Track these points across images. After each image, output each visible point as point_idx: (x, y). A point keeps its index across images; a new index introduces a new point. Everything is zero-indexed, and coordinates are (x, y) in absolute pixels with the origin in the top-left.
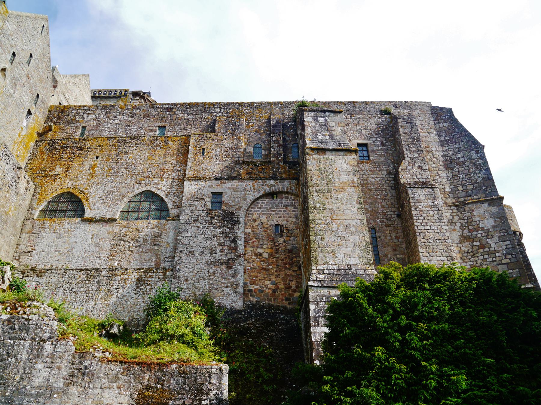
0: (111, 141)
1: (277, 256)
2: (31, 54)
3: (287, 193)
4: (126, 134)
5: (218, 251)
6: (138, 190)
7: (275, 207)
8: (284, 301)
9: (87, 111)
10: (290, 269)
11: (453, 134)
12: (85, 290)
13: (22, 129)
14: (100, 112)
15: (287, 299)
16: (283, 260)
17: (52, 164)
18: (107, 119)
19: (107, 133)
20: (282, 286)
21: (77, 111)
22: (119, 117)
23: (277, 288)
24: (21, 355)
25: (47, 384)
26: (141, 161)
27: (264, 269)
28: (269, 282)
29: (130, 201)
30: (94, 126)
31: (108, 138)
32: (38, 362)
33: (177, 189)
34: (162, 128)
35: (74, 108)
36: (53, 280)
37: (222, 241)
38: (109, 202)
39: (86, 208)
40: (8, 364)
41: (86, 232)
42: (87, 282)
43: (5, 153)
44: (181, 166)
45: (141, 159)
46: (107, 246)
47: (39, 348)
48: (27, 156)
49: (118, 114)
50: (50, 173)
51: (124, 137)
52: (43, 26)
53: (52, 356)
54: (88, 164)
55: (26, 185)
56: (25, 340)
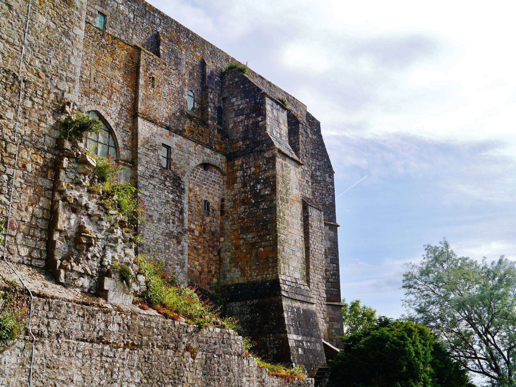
1: (204, 236)
3: (217, 168)
5: (171, 221)
7: (206, 181)
8: (207, 285)
10: (212, 253)
11: (317, 150)
15: (209, 284)
16: (208, 242)
20: (206, 270)
23: (203, 270)
27: (195, 248)
28: (197, 263)
33: (126, 122)
37: (174, 211)
44: (128, 90)
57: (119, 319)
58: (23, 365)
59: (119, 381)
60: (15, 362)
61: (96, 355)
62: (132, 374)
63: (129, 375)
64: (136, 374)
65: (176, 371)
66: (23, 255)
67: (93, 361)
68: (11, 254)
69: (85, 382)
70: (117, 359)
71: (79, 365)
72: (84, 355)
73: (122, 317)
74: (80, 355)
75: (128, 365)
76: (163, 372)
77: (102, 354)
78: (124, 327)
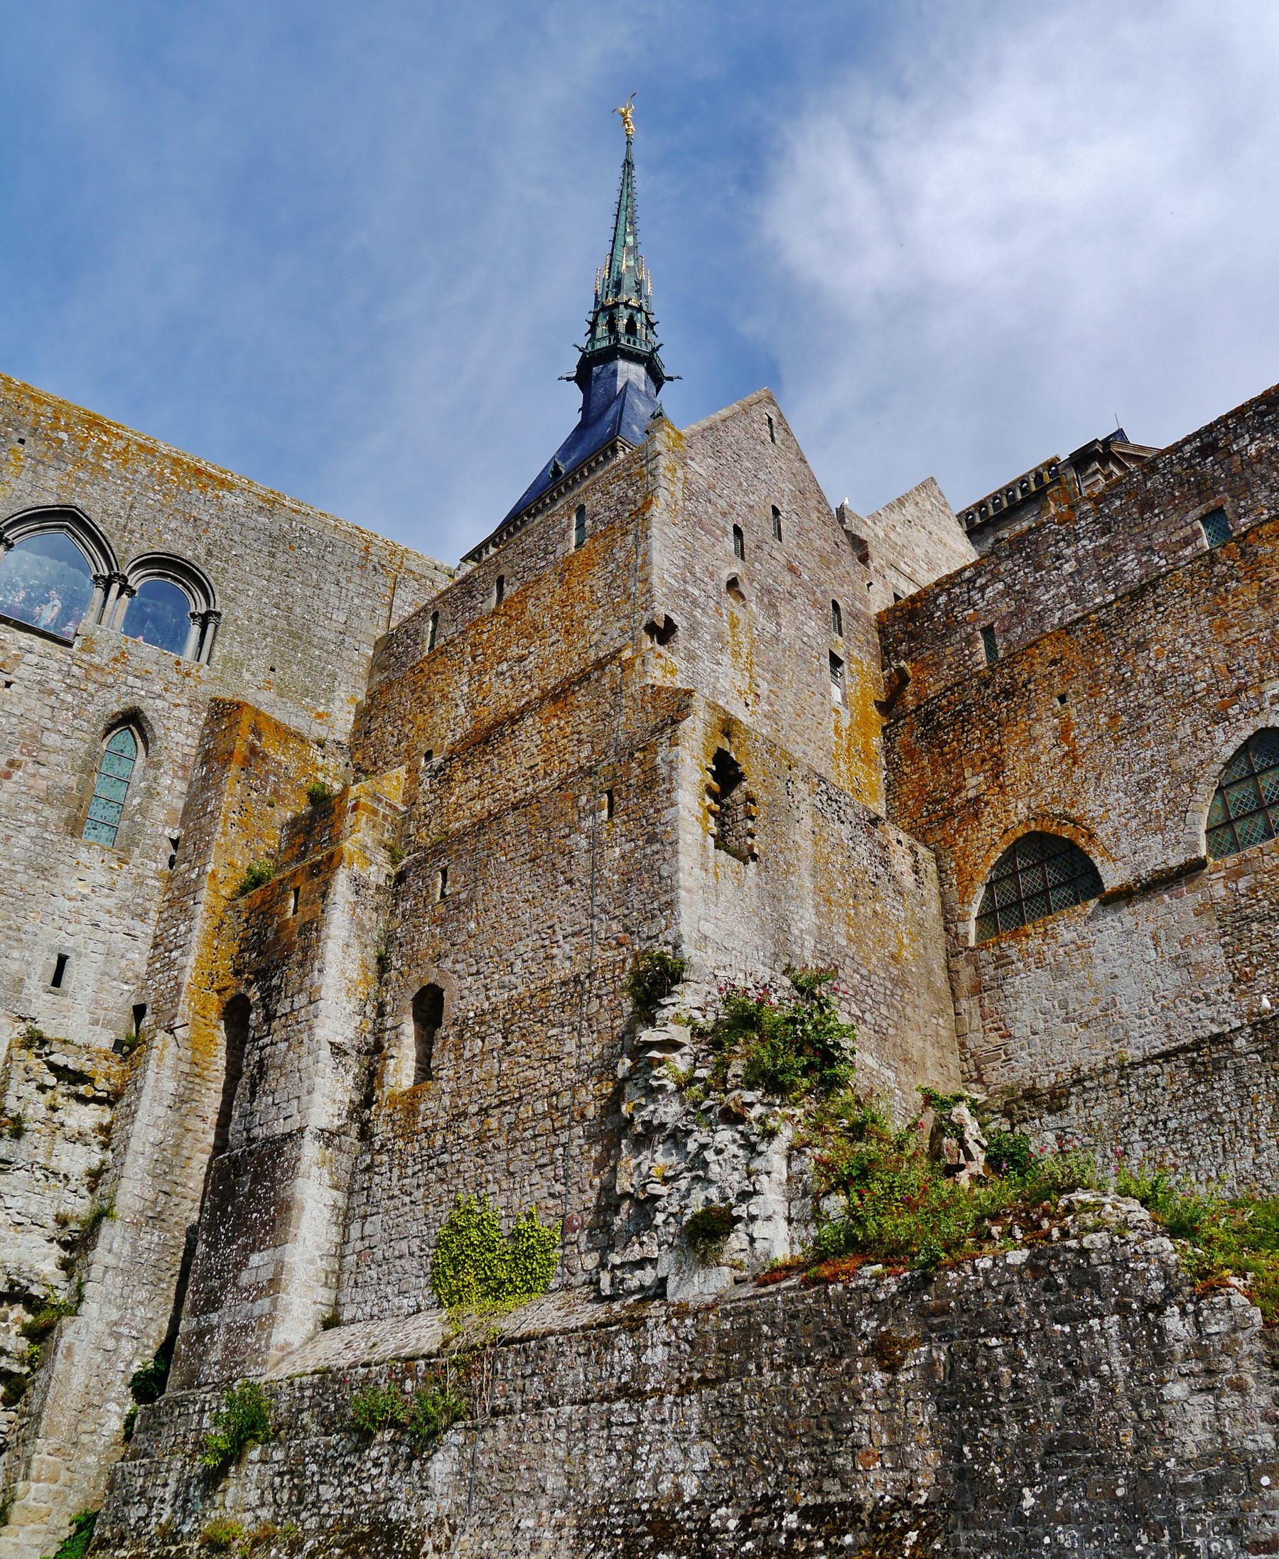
0: (1079, 633)
2: (774, 507)
4: (1114, 591)
6: (1227, 743)
9: (974, 582)
12: (1206, 1114)
13: (837, 712)
14: (1011, 565)
17: (950, 773)
18: (1037, 575)
19: (1058, 614)
21: (949, 595)
22: (1068, 552)
24: (1109, 1364)
25: (1224, 1443)
26: (1197, 650)
29: (1220, 790)
30: (1012, 614)
31: (1067, 629)
32: (1167, 1377)
34: (1213, 517)
35: (937, 591)
36: (1098, 1110)
38: (1158, 817)
39: (1097, 862)
40: (1083, 1400)
41: (1129, 933)
42: (1201, 1088)
43: (826, 797)
45: (1194, 645)
46: (1210, 953)
47: (1150, 1335)
48: (878, 779)
49: (1061, 544)
50: (957, 801)
51: (1111, 603)
52: (770, 420)
53: (1199, 1350)
54: (1045, 730)
55: (909, 860)
56: (1101, 1317)
57: (665, 1335)
58: (461, 1474)
59: (648, 1475)
60: (449, 1470)
61: (596, 1426)
62: (685, 1452)
63: (677, 1456)
64: (695, 1450)
65: (825, 1419)
66: (590, 1267)
67: (592, 1442)
68: (573, 1274)
69: (570, 1487)
70: (646, 1424)
71: (561, 1454)
72: (570, 1433)
73: (672, 1327)
74: (562, 1435)
75: (674, 1432)
76: (778, 1433)
77: (609, 1421)
78: (678, 1347)
